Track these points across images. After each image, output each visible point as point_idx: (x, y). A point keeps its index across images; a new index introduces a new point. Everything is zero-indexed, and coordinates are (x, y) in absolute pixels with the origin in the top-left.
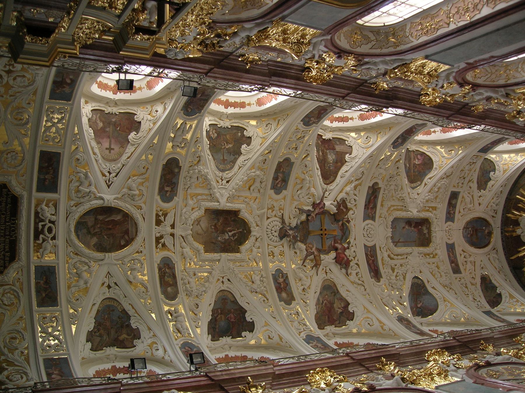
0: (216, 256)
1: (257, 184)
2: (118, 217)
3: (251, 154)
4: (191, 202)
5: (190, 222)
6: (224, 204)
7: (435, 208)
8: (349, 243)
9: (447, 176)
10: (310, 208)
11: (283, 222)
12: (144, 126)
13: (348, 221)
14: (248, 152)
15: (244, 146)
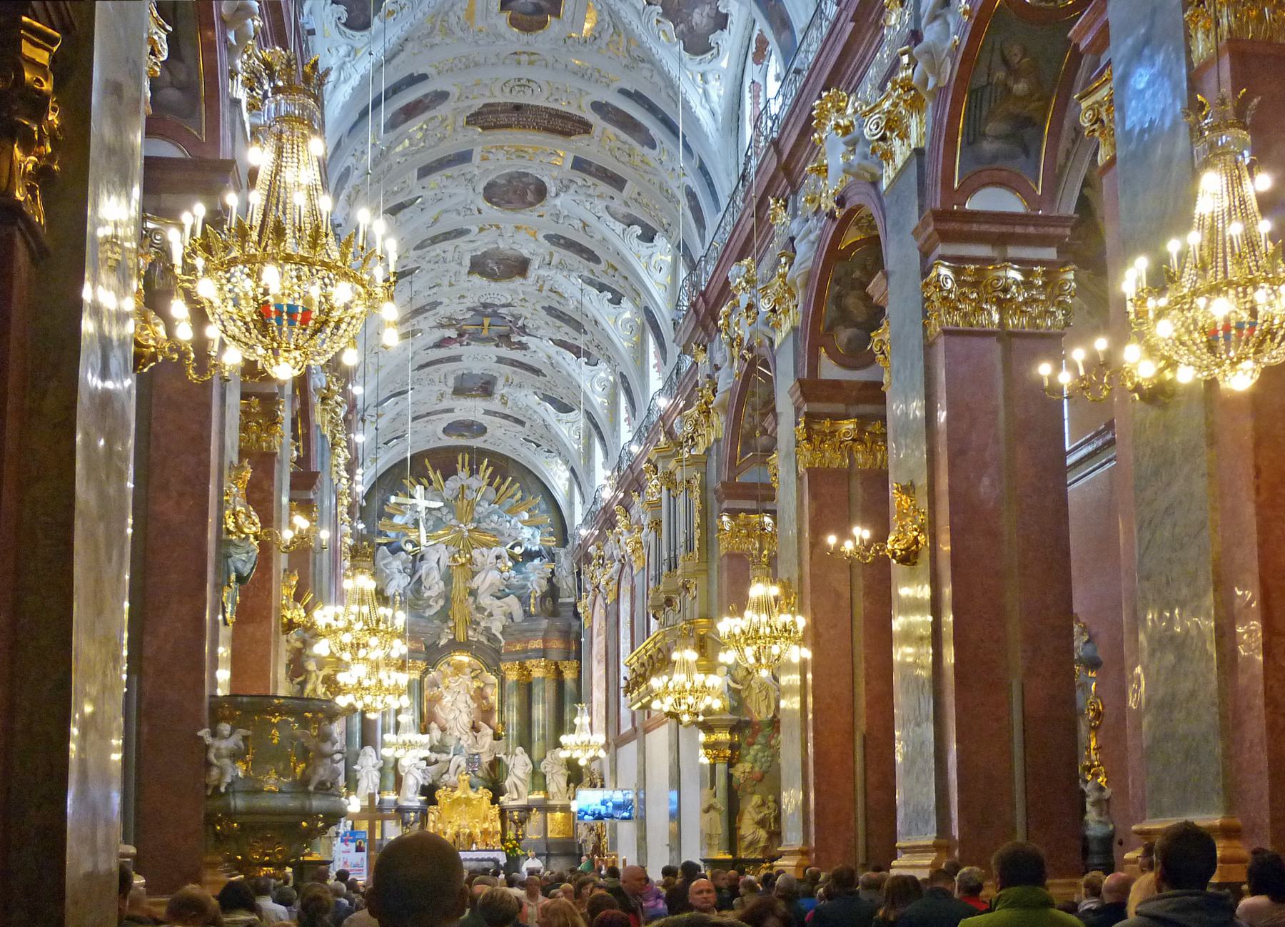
0: (467, 262)
1: (558, 298)
2: (530, 197)
3: (596, 305)
4: (542, 251)
5: (515, 246)
6: (533, 272)
7: (505, 404)
8: (468, 344)
9: (546, 426)
10: (520, 323)
11: (503, 306)
12: (644, 248)
13: (497, 346)
14: (600, 301)
15: (609, 296)
